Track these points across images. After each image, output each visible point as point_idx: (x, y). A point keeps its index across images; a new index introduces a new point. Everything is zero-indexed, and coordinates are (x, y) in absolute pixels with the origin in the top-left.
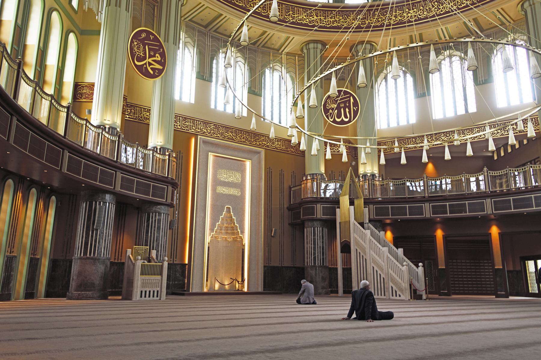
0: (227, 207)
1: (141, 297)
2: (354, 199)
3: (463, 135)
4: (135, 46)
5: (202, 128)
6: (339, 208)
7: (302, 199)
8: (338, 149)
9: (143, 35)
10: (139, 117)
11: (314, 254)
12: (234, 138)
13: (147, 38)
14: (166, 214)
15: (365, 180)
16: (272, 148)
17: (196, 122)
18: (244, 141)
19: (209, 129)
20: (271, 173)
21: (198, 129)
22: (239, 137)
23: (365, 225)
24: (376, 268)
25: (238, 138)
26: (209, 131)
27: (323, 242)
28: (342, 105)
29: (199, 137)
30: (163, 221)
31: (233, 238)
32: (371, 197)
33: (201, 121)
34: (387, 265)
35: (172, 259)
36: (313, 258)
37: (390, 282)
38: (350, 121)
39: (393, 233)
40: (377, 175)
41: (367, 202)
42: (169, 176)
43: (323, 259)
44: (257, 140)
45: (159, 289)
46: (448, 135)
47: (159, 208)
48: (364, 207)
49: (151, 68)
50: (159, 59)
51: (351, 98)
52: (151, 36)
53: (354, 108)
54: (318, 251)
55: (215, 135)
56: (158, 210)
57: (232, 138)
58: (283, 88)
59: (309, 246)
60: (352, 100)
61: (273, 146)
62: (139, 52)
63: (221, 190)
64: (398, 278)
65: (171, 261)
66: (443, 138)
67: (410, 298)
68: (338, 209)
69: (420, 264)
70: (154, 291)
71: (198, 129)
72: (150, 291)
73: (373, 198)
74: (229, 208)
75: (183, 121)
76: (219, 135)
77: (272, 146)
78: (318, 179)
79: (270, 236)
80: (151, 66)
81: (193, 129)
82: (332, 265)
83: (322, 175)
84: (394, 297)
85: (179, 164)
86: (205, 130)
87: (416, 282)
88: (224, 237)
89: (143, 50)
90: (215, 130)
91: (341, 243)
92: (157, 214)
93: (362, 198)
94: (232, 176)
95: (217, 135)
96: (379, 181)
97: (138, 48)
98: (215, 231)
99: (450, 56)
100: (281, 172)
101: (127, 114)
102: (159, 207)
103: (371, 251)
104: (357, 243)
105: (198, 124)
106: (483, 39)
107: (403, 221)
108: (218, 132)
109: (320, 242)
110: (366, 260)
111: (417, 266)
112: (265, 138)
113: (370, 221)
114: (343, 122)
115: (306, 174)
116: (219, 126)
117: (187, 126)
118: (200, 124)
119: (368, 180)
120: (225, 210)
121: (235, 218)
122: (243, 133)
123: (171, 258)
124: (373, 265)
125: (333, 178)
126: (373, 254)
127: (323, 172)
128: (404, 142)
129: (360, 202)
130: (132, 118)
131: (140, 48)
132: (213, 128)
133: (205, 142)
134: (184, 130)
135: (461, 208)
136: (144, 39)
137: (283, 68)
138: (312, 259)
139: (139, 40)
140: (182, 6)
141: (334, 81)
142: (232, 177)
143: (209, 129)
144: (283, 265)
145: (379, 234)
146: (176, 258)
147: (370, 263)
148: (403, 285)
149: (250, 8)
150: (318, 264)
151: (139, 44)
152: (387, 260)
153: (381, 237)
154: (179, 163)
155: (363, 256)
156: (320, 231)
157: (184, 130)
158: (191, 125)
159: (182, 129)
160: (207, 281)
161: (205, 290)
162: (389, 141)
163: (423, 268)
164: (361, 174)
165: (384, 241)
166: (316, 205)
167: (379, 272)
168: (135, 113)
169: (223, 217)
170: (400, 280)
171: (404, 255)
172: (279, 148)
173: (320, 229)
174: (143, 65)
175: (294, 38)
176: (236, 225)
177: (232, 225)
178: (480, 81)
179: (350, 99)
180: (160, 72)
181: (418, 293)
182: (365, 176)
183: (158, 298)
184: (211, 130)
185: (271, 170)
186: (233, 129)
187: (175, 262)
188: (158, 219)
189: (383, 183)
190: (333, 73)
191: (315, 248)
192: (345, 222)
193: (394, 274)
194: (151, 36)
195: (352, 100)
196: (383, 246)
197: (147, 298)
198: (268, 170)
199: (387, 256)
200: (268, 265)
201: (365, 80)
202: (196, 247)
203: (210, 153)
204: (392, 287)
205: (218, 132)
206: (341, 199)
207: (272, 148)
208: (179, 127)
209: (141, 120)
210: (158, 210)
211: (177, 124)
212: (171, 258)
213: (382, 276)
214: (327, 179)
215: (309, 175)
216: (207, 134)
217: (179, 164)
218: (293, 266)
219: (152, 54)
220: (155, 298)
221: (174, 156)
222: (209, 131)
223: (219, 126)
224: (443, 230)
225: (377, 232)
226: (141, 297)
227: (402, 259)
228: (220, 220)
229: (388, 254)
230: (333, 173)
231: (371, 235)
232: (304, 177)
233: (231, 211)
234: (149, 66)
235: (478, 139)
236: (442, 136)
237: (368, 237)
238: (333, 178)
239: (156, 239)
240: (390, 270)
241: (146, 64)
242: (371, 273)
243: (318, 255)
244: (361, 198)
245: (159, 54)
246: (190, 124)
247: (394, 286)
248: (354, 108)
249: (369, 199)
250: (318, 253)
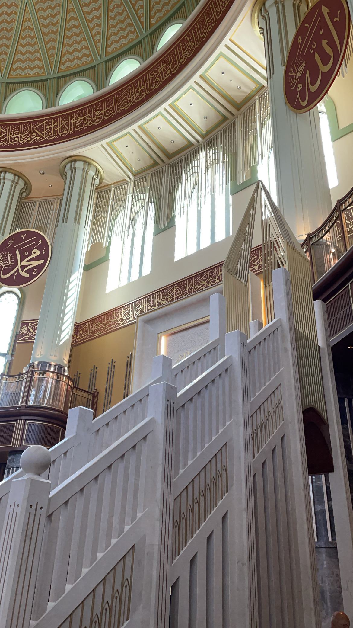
17: (153, 297)
44: (254, 261)
49: (26, 272)
50: (38, 253)
52: (22, 236)
75: (136, 306)
108: (183, 292)
131: (7, 258)
136: (13, 244)
174: (14, 273)
184: (173, 296)
186: (207, 271)
194: (22, 236)
205: (183, 292)
241: (17, 271)
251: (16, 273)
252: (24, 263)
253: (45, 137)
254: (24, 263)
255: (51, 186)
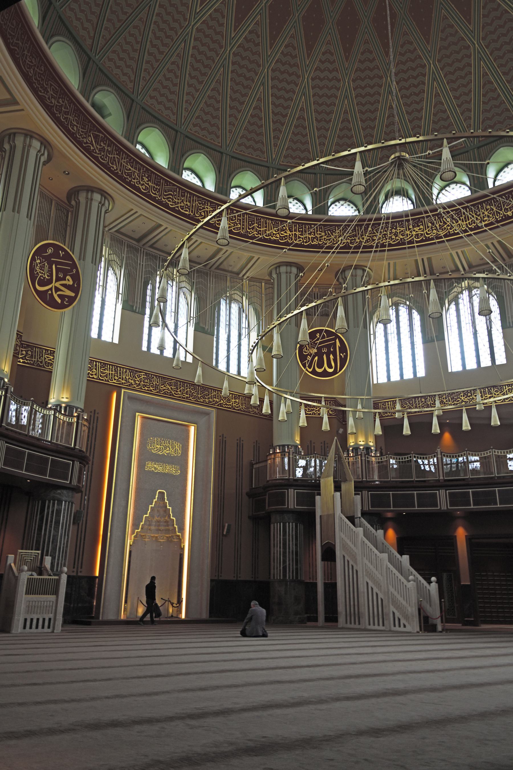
0: (159, 492)
1: (25, 627)
2: (341, 482)
3: (490, 396)
4: (37, 265)
5: (128, 378)
6: (319, 494)
7: (268, 481)
8: (319, 411)
9: (50, 251)
10: (38, 361)
11: (284, 562)
12: (173, 392)
13: (55, 254)
14: (69, 502)
15: (357, 454)
16: (227, 408)
17: (120, 370)
18: (187, 397)
19: (138, 379)
20: (225, 443)
21: (123, 380)
22: (180, 391)
23: (356, 520)
24: (371, 584)
25: (179, 393)
26: (138, 383)
27: (296, 545)
28: (325, 350)
29: (123, 390)
30: (64, 513)
31: (167, 537)
32: (364, 479)
33: (127, 369)
34: (387, 580)
35: (75, 570)
36: (283, 568)
37: (391, 606)
38: (335, 372)
39: (396, 531)
40: (372, 448)
41: (359, 487)
42: (77, 447)
43: (297, 569)
45: (51, 616)
46: (469, 394)
47: (60, 494)
48: (355, 494)
49: (59, 296)
50: (71, 283)
51: (337, 340)
53: (341, 354)
54: (289, 558)
55: (146, 389)
56: (58, 496)
57: (171, 392)
58: (244, 324)
59: (277, 550)
60: (338, 344)
61: (229, 405)
62: (42, 273)
63: (151, 466)
64: (401, 599)
65: (73, 572)
66: (463, 398)
67: (418, 630)
68: (319, 496)
69: (433, 579)
70: (44, 620)
71: (123, 380)
72: (38, 620)
73: (367, 482)
74: (164, 493)
75: (101, 368)
76: (151, 388)
77: (227, 405)
78: (291, 453)
79: (221, 535)
80: (59, 293)
81: (115, 380)
82: (310, 578)
83: (296, 447)
84: (397, 628)
85: (93, 429)
86: (132, 381)
87: (428, 606)
88: (154, 536)
89: (49, 271)
90: (146, 381)
91: (322, 547)
92: (56, 502)
93: (351, 481)
94: (169, 447)
95: (149, 388)
96: (376, 456)
97: (42, 268)
98: (140, 527)
99: (470, 289)
100: (238, 441)
101: (22, 358)
102: (59, 491)
103: (365, 559)
104: (344, 546)
105: (123, 372)
106: (498, 275)
107: (409, 514)
108: (150, 384)
109: (293, 544)
110: (357, 571)
111: (430, 582)
112: (218, 393)
113: (363, 514)
114: (325, 374)
115: (275, 444)
116: (153, 376)
117: (107, 375)
118: (125, 372)
119: (361, 455)
120: (157, 496)
121: (171, 508)
122: (187, 386)
123: (74, 568)
124: (367, 579)
125: (313, 453)
126: (367, 562)
127: (298, 442)
128: (409, 403)
129: (349, 487)
130: (27, 363)
131: (44, 267)
132: (144, 378)
133: (131, 398)
134: (102, 380)
135: (489, 498)
136: (51, 255)
137: (244, 298)
138: (280, 570)
139: (44, 257)
140: (106, 212)
141: (304, 323)
142: (168, 449)
143: (138, 379)
144: (239, 579)
145: (375, 534)
146: (81, 568)
147: (363, 577)
148: (409, 609)
149: (199, 218)
150: (289, 577)
151: (43, 262)
152: (387, 572)
153: (378, 538)
154: (93, 427)
155: (352, 566)
156: (292, 528)
157: (102, 380)
158: (112, 374)
159: (100, 379)
160: (126, 602)
161: (122, 617)
162: (390, 401)
163: (437, 584)
164: (350, 446)
165: (383, 544)
166: (288, 489)
167: (375, 590)
168: (32, 356)
169: (153, 506)
170: (404, 603)
171: (411, 565)
172: (237, 407)
173: (292, 525)
174: (48, 290)
175: (259, 258)
176: (172, 518)
177: (166, 518)
178: (509, 323)
179: (336, 342)
180: (72, 300)
181: (431, 621)
182: (356, 449)
183: (50, 630)
184: (141, 382)
185: (224, 439)
186: (172, 380)
187: (79, 574)
188: (57, 510)
189: (381, 459)
190: (304, 314)
191: (285, 553)
192: (328, 516)
193: (396, 593)
195: (338, 344)
196: (382, 552)
197: (34, 630)
198: (221, 438)
199: (387, 566)
200: (216, 578)
201: (346, 324)
202: (112, 551)
203: (137, 414)
204: (394, 613)
205: (150, 384)
206: (322, 481)
207: (227, 408)
208: (94, 376)
209: (41, 366)
210: (58, 496)
211: (93, 372)
212: (74, 568)
213: (380, 596)
214: (304, 453)
215: (278, 447)
216: (134, 387)
217: (93, 429)
218: (253, 579)
219: (61, 275)
220: (46, 630)
221: (85, 418)
222: (138, 383)
223: (153, 376)
224: (466, 529)
225: (373, 531)
226: (25, 627)
227: (407, 571)
228: (149, 511)
229: (388, 563)
230: (313, 445)
231: (364, 535)
232: (271, 450)
233: (166, 497)
234: (56, 293)
235: (509, 401)
236: (461, 396)
237: (360, 538)
238: (313, 453)
239: (53, 540)
240: (390, 587)
241: (51, 289)
242: (364, 592)
243: (289, 564)
244: (351, 481)
245: (70, 275)
246: (111, 372)
247: (396, 612)
248: (341, 354)
249: (362, 482)
250: (289, 560)
251: (50, 292)
252: (58, 284)
253: (98, 154)
254: (58, 284)
255: (52, 179)
